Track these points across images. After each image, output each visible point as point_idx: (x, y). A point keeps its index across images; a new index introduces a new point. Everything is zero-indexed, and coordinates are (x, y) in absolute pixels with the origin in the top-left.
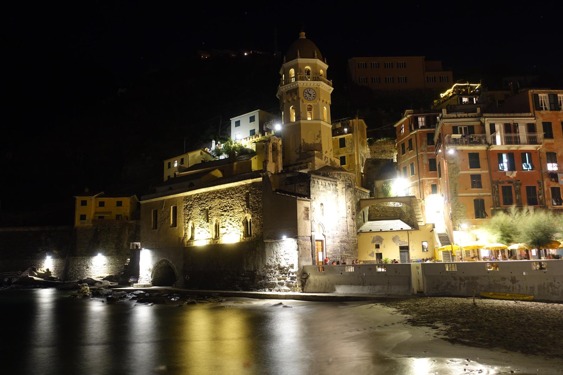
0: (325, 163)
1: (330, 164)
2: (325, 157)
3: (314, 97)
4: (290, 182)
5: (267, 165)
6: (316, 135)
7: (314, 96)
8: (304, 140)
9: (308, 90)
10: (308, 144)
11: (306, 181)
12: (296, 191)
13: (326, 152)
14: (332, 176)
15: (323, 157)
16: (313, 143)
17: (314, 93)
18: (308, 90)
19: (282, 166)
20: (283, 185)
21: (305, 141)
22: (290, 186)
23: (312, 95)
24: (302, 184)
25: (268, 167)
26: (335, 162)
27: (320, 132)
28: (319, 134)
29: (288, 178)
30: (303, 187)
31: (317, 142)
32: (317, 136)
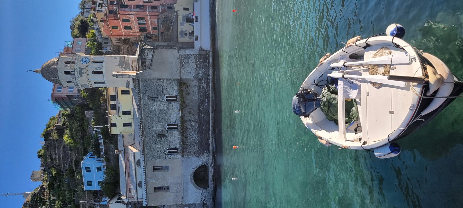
11: (145, 51)
21: (117, 65)
22: (147, 64)
24: (146, 54)
30: (148, 54)
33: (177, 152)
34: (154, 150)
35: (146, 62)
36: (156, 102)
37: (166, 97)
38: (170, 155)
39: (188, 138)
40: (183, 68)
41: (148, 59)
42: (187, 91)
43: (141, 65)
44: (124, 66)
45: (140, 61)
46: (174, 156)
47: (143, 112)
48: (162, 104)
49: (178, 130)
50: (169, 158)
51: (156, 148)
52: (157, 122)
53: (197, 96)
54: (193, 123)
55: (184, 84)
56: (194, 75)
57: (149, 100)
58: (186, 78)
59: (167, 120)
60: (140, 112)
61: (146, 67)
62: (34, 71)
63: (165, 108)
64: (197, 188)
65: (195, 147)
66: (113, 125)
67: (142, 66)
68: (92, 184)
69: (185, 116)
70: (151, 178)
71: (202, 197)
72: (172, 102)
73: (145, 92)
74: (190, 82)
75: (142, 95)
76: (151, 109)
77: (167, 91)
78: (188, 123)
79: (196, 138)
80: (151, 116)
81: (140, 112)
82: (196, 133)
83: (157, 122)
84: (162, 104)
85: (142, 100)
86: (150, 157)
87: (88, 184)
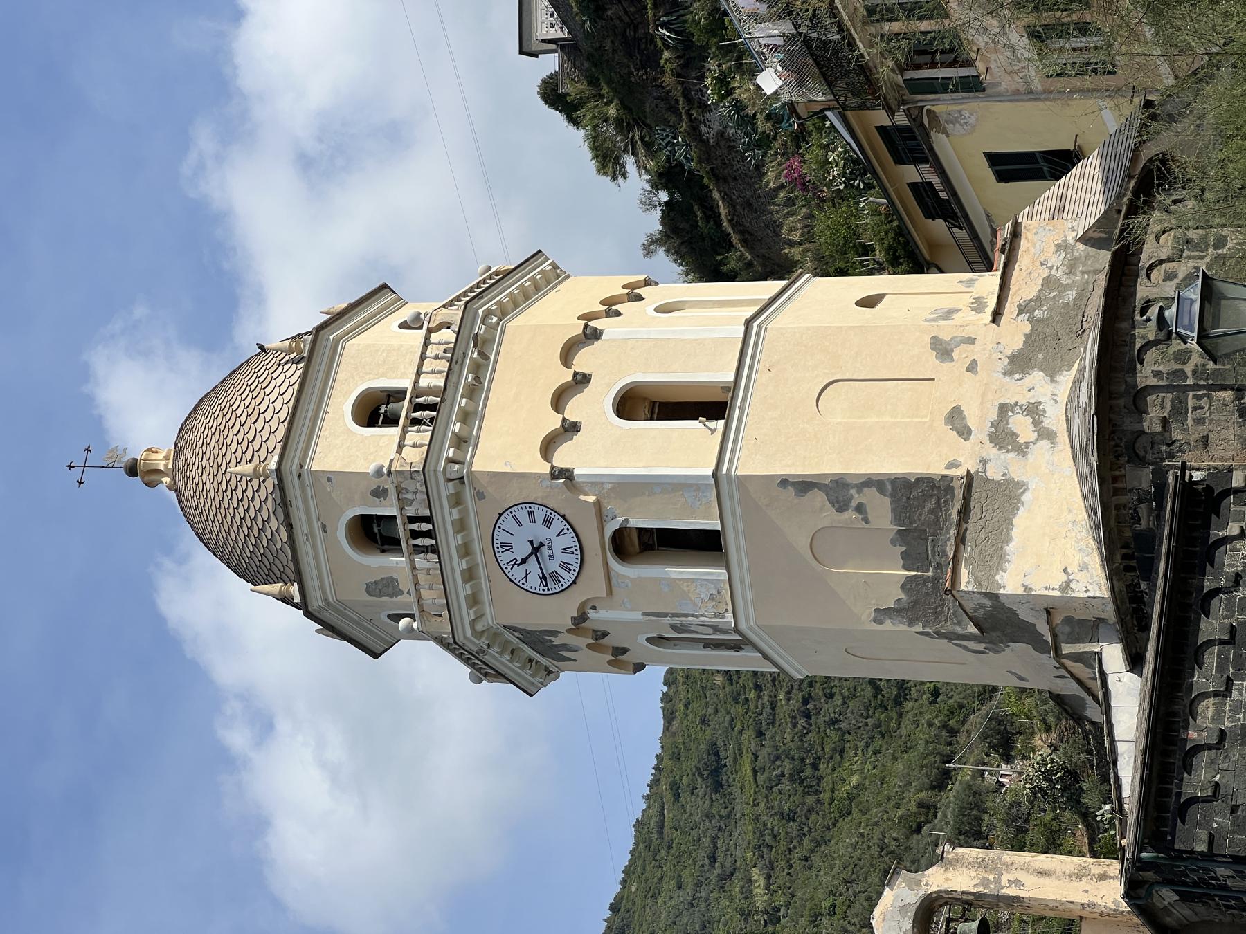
0: (1045, 443)
1: (1052, 374)
2: (1002, 437)
3: (548, 522)
6: (829, 515)
7: (540, 514)
8: (881, 614)
9: (506, 557)
10: (910, 579)
13: (956, 419)
14: (1143, 509)
15: (1000, 465)
16: (893, 542)
17: (522, 514)
18: (506, 557)
23: (541, 533)
26: (1039, 300)
27: (804, 485)
28: (818, 497)
31: (881, 510)
32: (842, 507)
44: (972, 629)
62: (132, 470)
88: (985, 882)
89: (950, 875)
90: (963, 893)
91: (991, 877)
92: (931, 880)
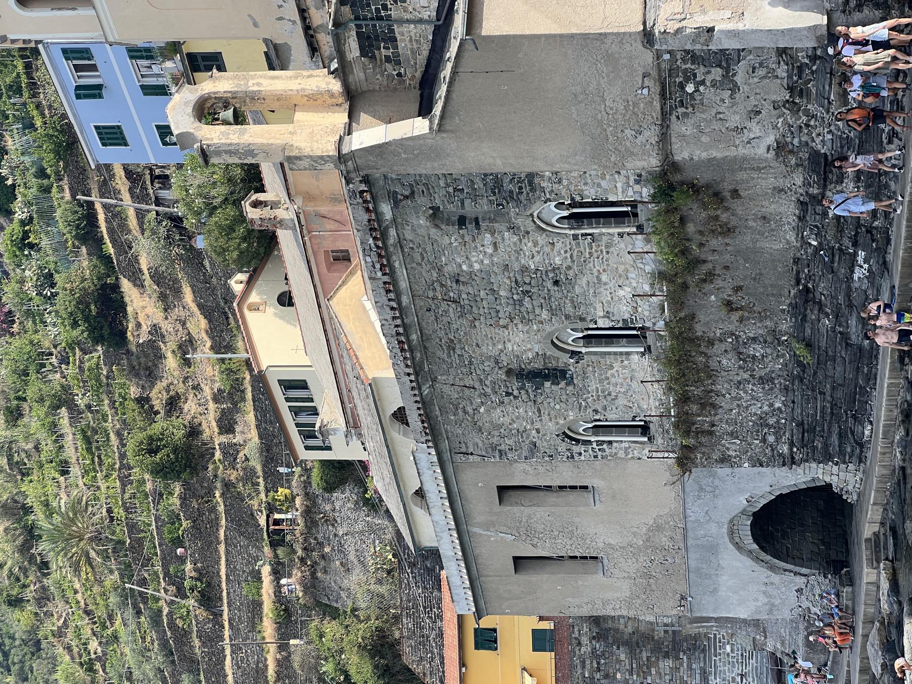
4: (382, 45)
5: (307, 151)
12: (426, 17)
19: (305, 73)
20: (399, 75)
22: (401, 45)
25: (315, 146)
29: (363, 53)
33: (645, 429)
34: (499, 427)
35: (399, 37)
36: (488, 236)
37: (560, 206)
38: (600, 443)
39: (714, 406)
40: (681, 110)
41: (409, 21)
42: (716, 218)
43: (362, 55)
45: (354, 33)
46: (626, 449)
47: (403, 284)
48: (536, 244)
49: (648, 349)
50: (596, 457)
51: (507, 420)
52: (501, 322)
53: (791, 236)
54: (757, 350)
55: (695, 189)
56: (770, 139)
57: (437, 226)
58: (710, 160)
59: (569, 309)
60: (386, 279)
61: (398, 63)
63: (558, 261)
64: (772, 568)
65: (764, 440)
66: (202, 64)
67: (373, 57)
68: (124, 138)
69: (702, 317)
70: (487, 526)
71: (806, 604)
72: (604, 230)
73: (407, 193)
74: (742, 176)
75: (386, 209)
76: (460, 266)
77: (565, 182)
78: (718, 348)
79: (771, 405)
80: (464, 296)
81: (386, 279)
82: (771, 389)
83: (501, 322)
84: (530, 244)
85: (392, 232)
86: (471, 450)
87: (101, 139)
88: (238, 85)
89: (216, 84)
90: (224, 92)
91: (242, 83)
92: (204, 88)
